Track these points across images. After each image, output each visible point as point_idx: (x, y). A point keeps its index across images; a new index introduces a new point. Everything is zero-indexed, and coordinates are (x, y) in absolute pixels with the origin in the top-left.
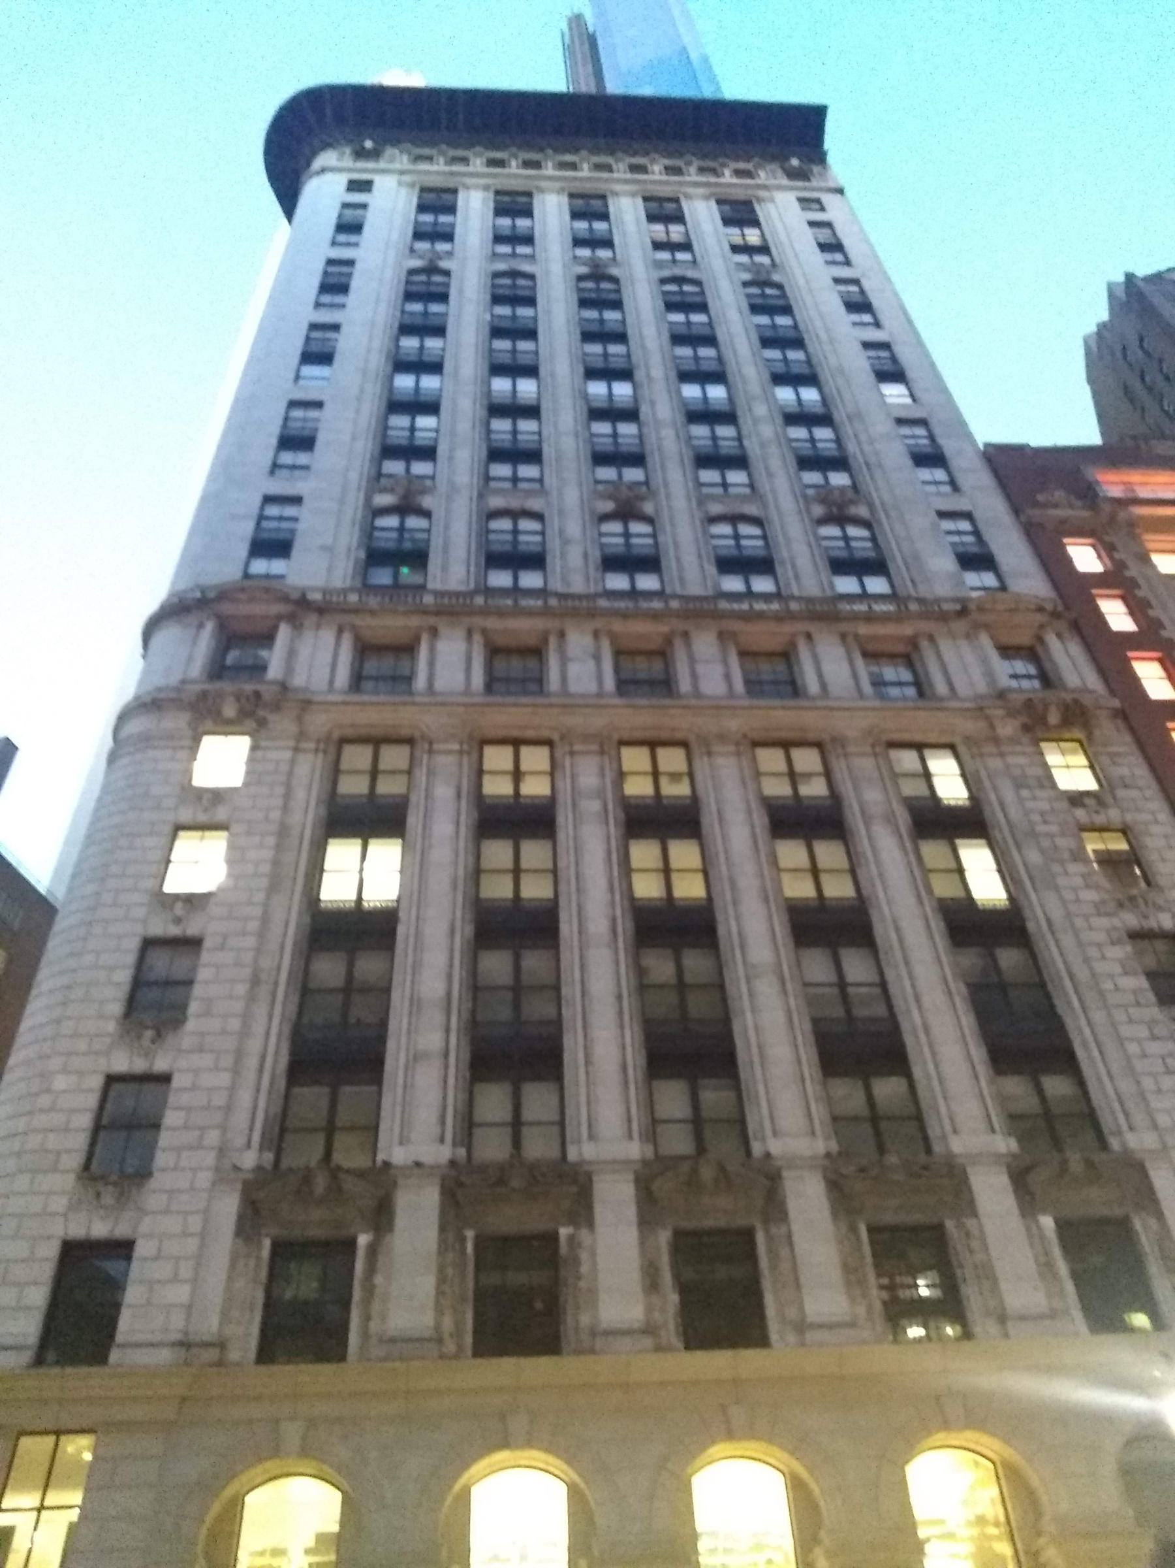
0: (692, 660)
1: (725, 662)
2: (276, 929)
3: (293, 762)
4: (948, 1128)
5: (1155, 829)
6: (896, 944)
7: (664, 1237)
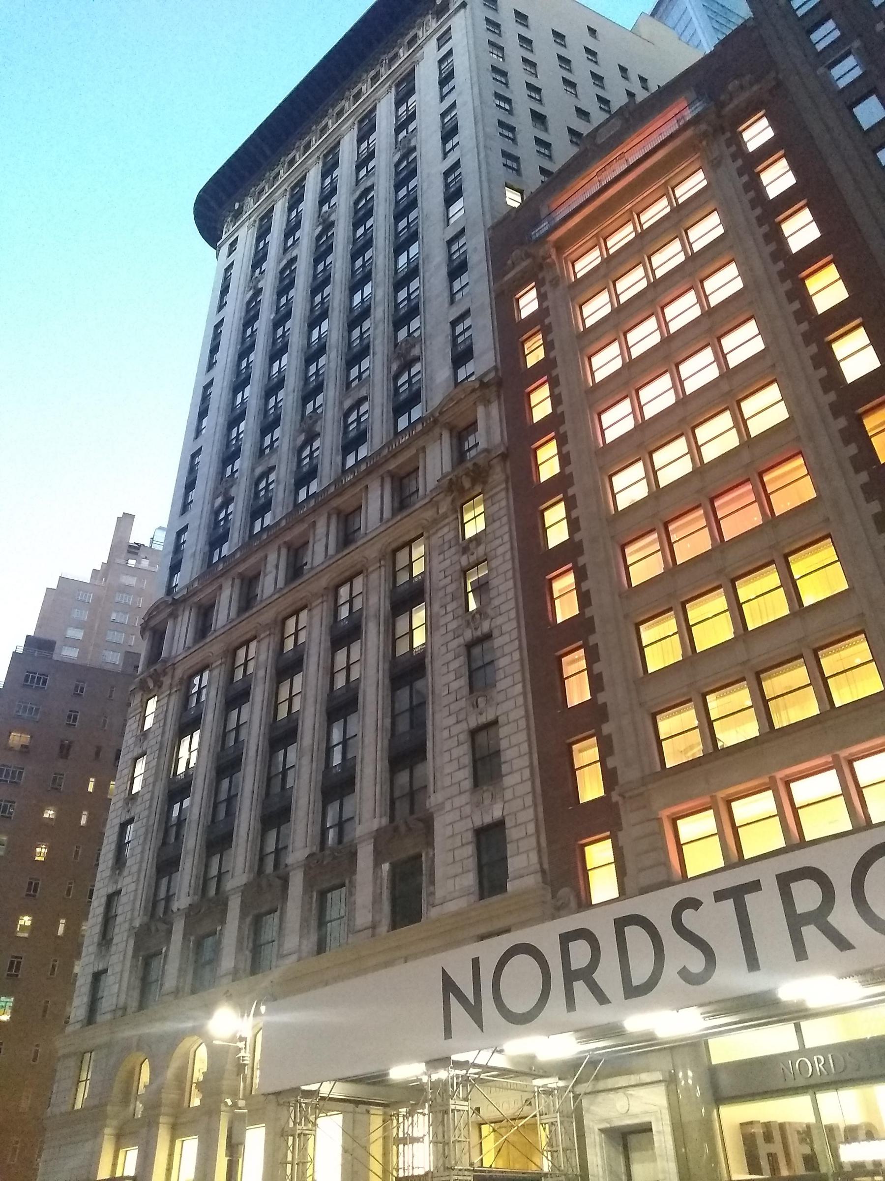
3: (168, 704)
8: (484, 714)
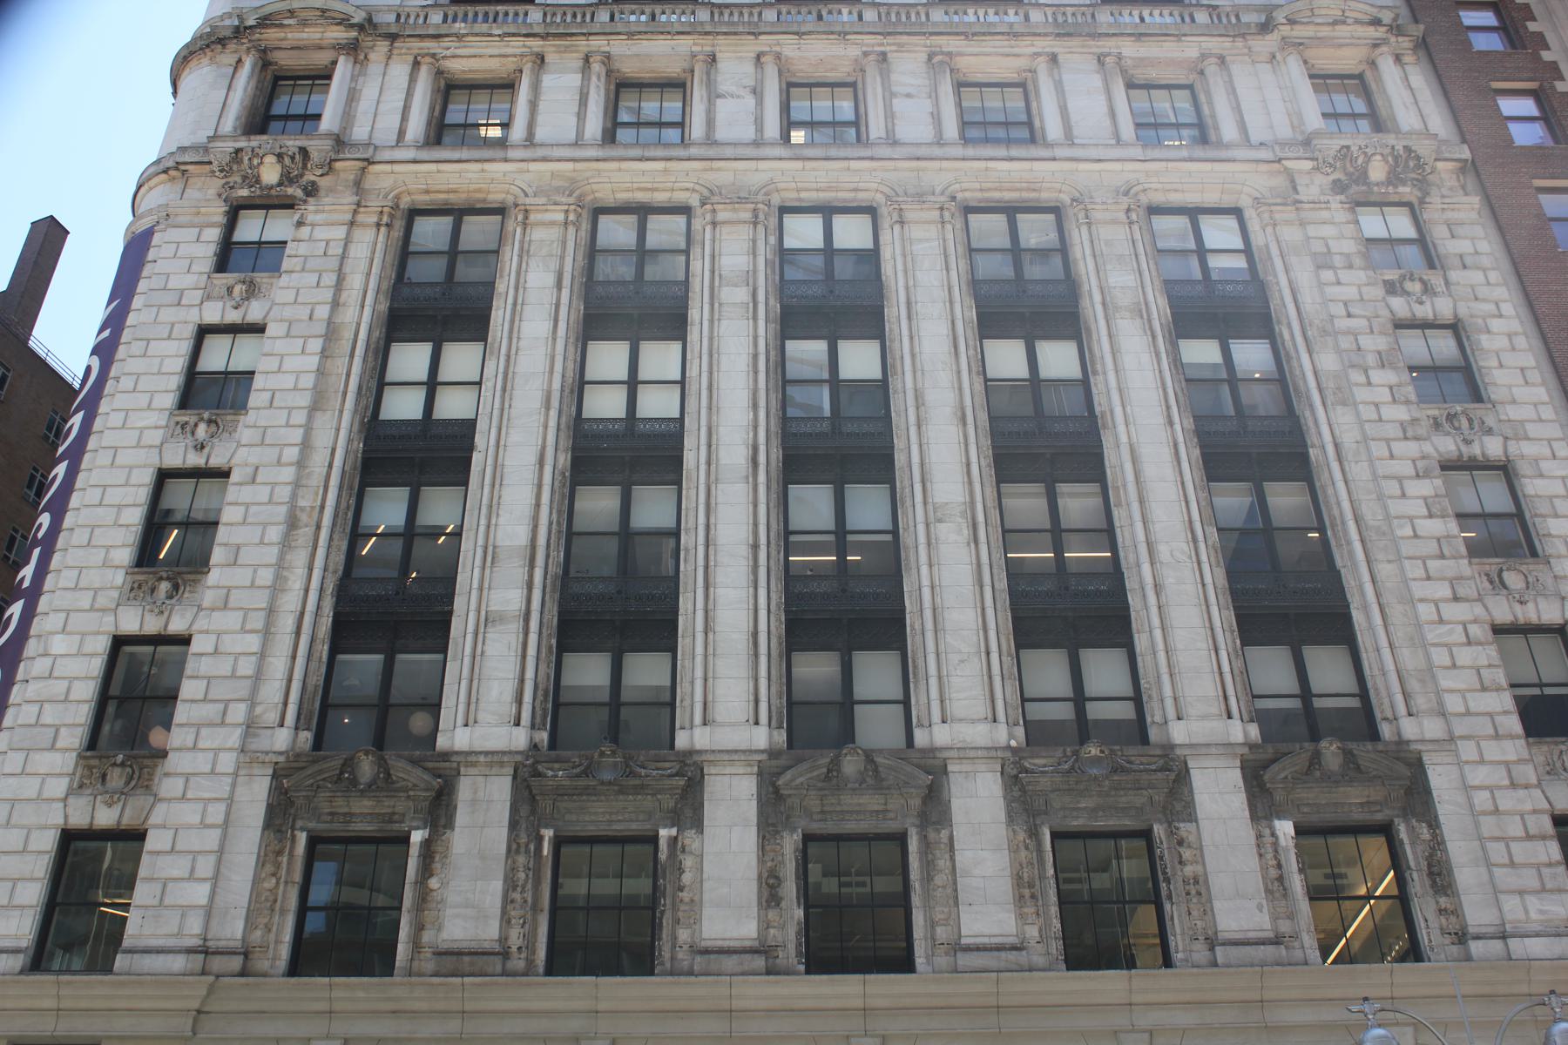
0: (889, 95)
1: (934, 95)
2: (319, 460)
3: (347, 241)
4: (1171, 713)
5: (1495, 324)
6: (1130, 477)
7: (790, 843)
8: (1531, 605)
